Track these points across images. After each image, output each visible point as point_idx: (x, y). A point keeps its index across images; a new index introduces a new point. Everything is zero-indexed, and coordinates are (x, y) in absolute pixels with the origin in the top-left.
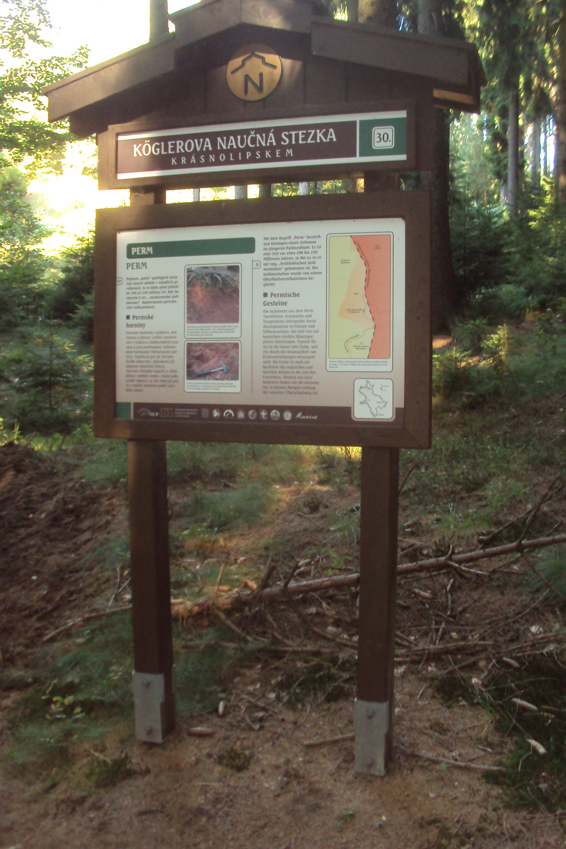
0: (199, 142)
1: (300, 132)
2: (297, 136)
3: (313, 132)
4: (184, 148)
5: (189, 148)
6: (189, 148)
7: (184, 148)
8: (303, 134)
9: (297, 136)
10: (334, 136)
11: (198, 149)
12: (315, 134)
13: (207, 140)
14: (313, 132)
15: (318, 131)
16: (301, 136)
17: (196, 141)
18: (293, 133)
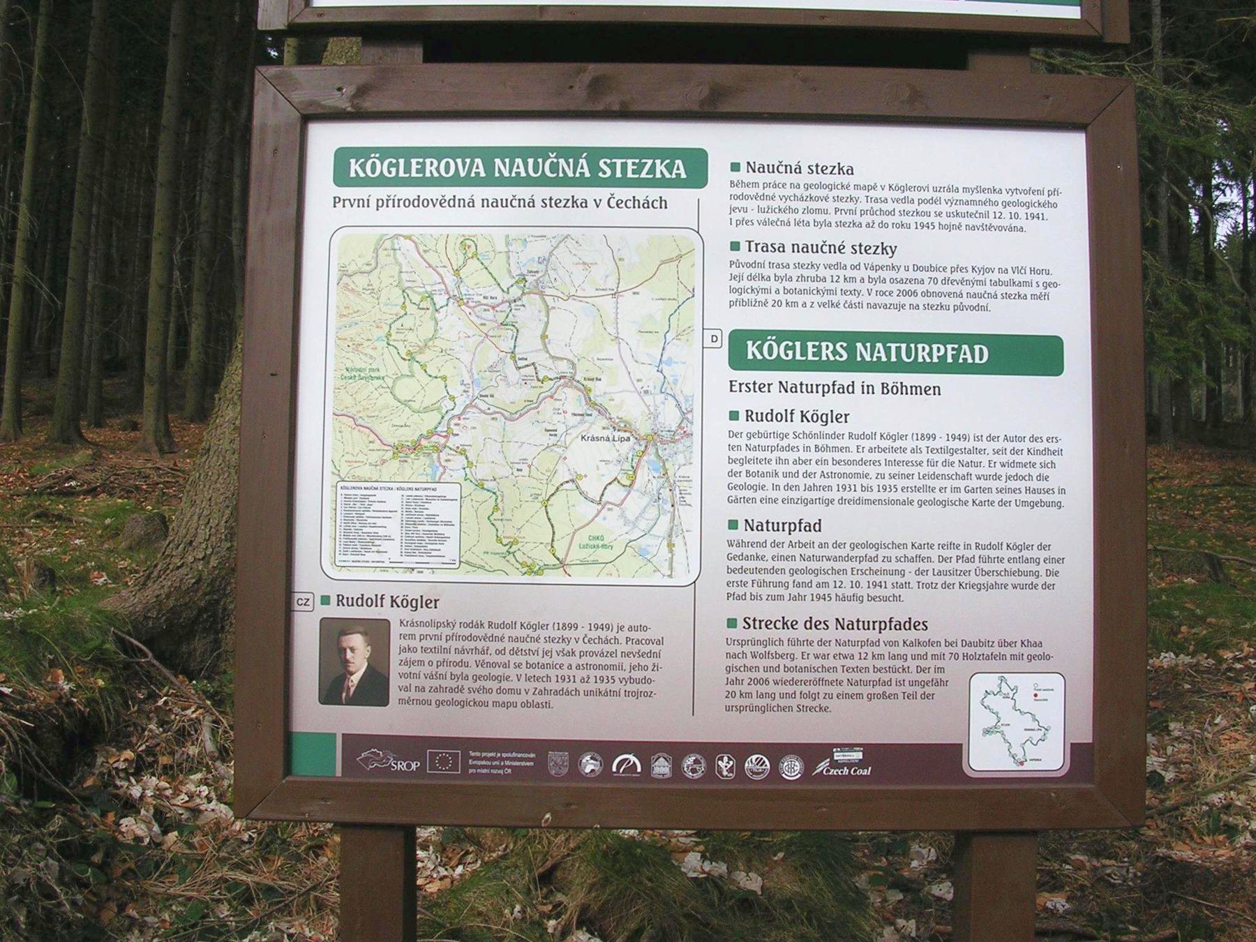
0: (464, 164)
1: (630, 162)
2: (624, 166)
3: (650, 162)
4: (438, 169)
5: (447, 171)
6: (447, 171)
7: (438, 169)
8: (634, 164)
9: (624, 166)
10: (682, 171)
11: (463, 174)
12: (654, 164)
13: (478, 161)
14: (650, 162)
15: (658, 162)
16: (630, 168)
17: (459, 161)
18: (619, 162)
